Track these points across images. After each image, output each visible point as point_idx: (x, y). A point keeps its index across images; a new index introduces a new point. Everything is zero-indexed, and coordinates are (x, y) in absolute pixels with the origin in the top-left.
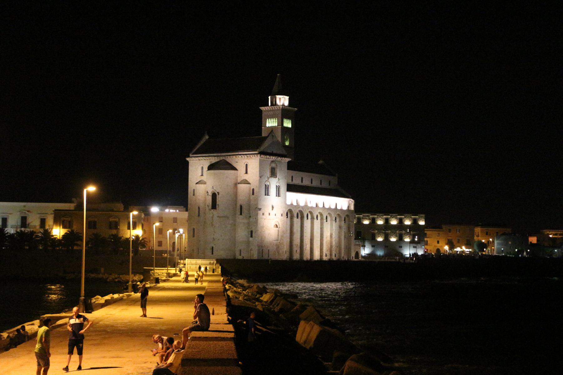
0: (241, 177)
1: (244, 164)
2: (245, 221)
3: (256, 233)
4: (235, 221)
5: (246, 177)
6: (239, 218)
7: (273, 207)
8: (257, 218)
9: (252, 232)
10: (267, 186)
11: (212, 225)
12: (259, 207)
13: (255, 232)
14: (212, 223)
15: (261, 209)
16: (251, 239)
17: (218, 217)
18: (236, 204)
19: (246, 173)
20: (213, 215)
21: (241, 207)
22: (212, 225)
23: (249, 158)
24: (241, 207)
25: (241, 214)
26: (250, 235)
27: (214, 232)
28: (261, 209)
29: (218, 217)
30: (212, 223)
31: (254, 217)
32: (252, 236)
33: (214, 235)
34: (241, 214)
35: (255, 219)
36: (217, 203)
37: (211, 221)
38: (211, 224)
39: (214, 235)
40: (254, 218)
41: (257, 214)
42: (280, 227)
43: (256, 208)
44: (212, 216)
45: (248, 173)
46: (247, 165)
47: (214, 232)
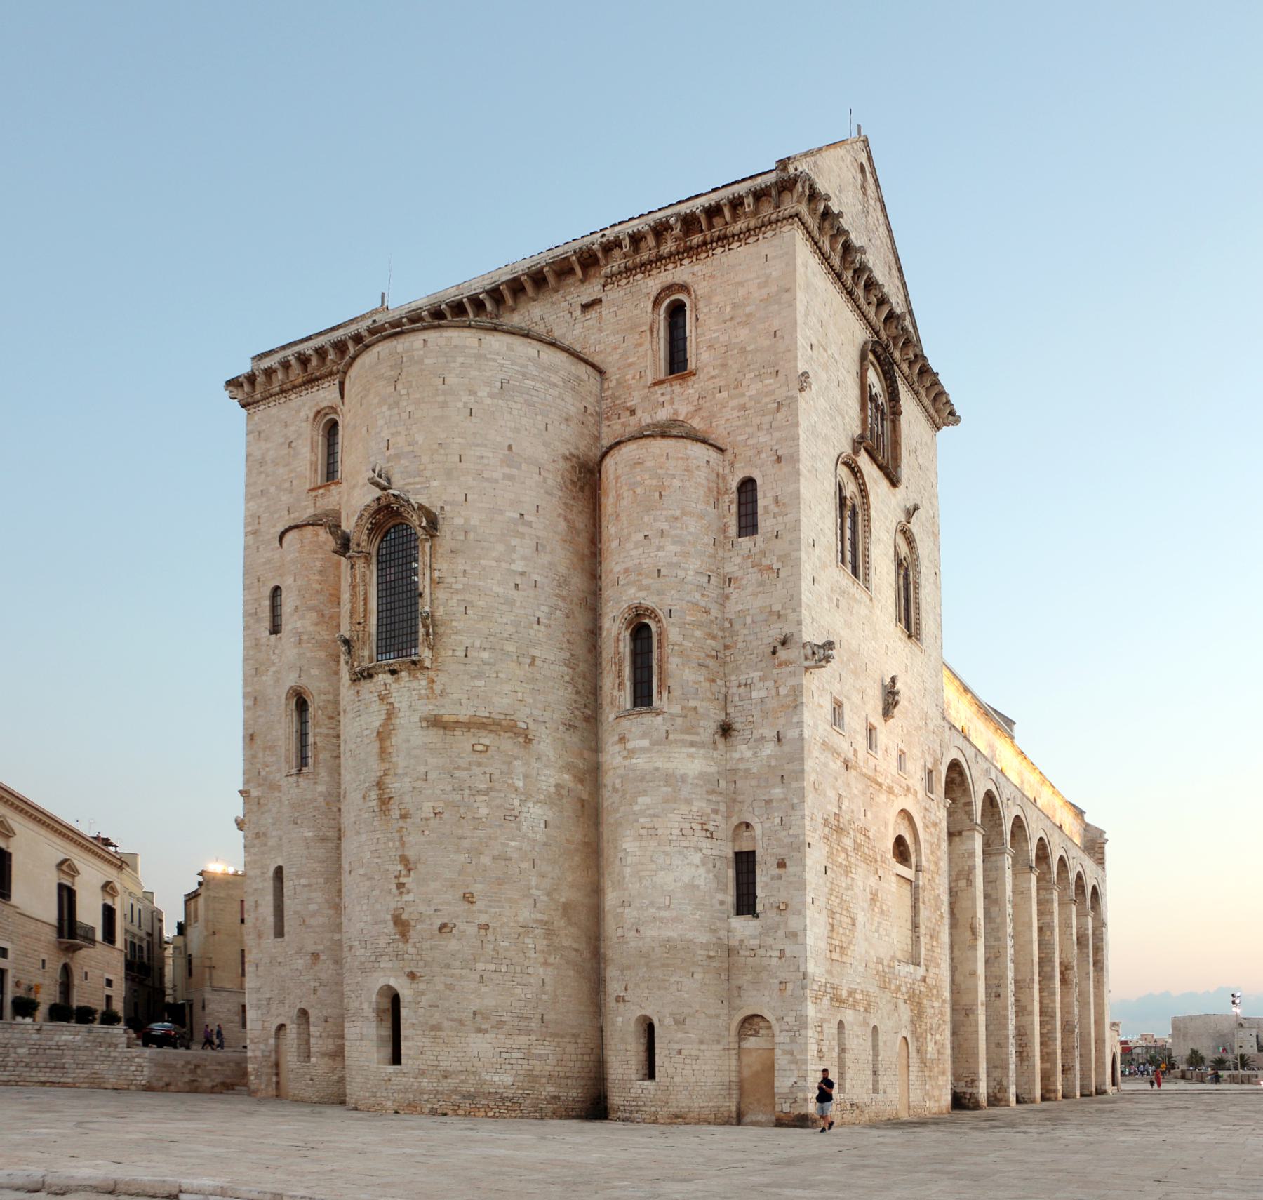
0: (633, 412)
1: (657, 303)
3: (791, 869)
6: (623, 739)
8: (792, 734)
9: (745, 863)
11: (384, 802)
12: (806, 638)
13: (782, 865)
14: (380, 785)
15: (829, 645)
16: (743, 926)
17: (435, 722)
18: (594, 632)
19: (677, 363)
20: (390, 715)
21: (641, 632)
22: (385, 802)
23: (696, 239)
24: (641, 632)
25: (642, 696)
26: (730, 898)
27: (404, 860)
28: (829, 645)
30: (380, 785)
31: (770, 733)
32: (746, 903)
33: (400, 886)
34: (642, 696)
35: (769, 749)
36: (425, 606)
37: (376, 767)
38: (374, 794)
39: (400, 886)
40: (762, 739)
41: (797, 691)
43: (784, 643)
44: (377, 721)
45: (691, 365)
46: (676, 313)
47: (404, 860)
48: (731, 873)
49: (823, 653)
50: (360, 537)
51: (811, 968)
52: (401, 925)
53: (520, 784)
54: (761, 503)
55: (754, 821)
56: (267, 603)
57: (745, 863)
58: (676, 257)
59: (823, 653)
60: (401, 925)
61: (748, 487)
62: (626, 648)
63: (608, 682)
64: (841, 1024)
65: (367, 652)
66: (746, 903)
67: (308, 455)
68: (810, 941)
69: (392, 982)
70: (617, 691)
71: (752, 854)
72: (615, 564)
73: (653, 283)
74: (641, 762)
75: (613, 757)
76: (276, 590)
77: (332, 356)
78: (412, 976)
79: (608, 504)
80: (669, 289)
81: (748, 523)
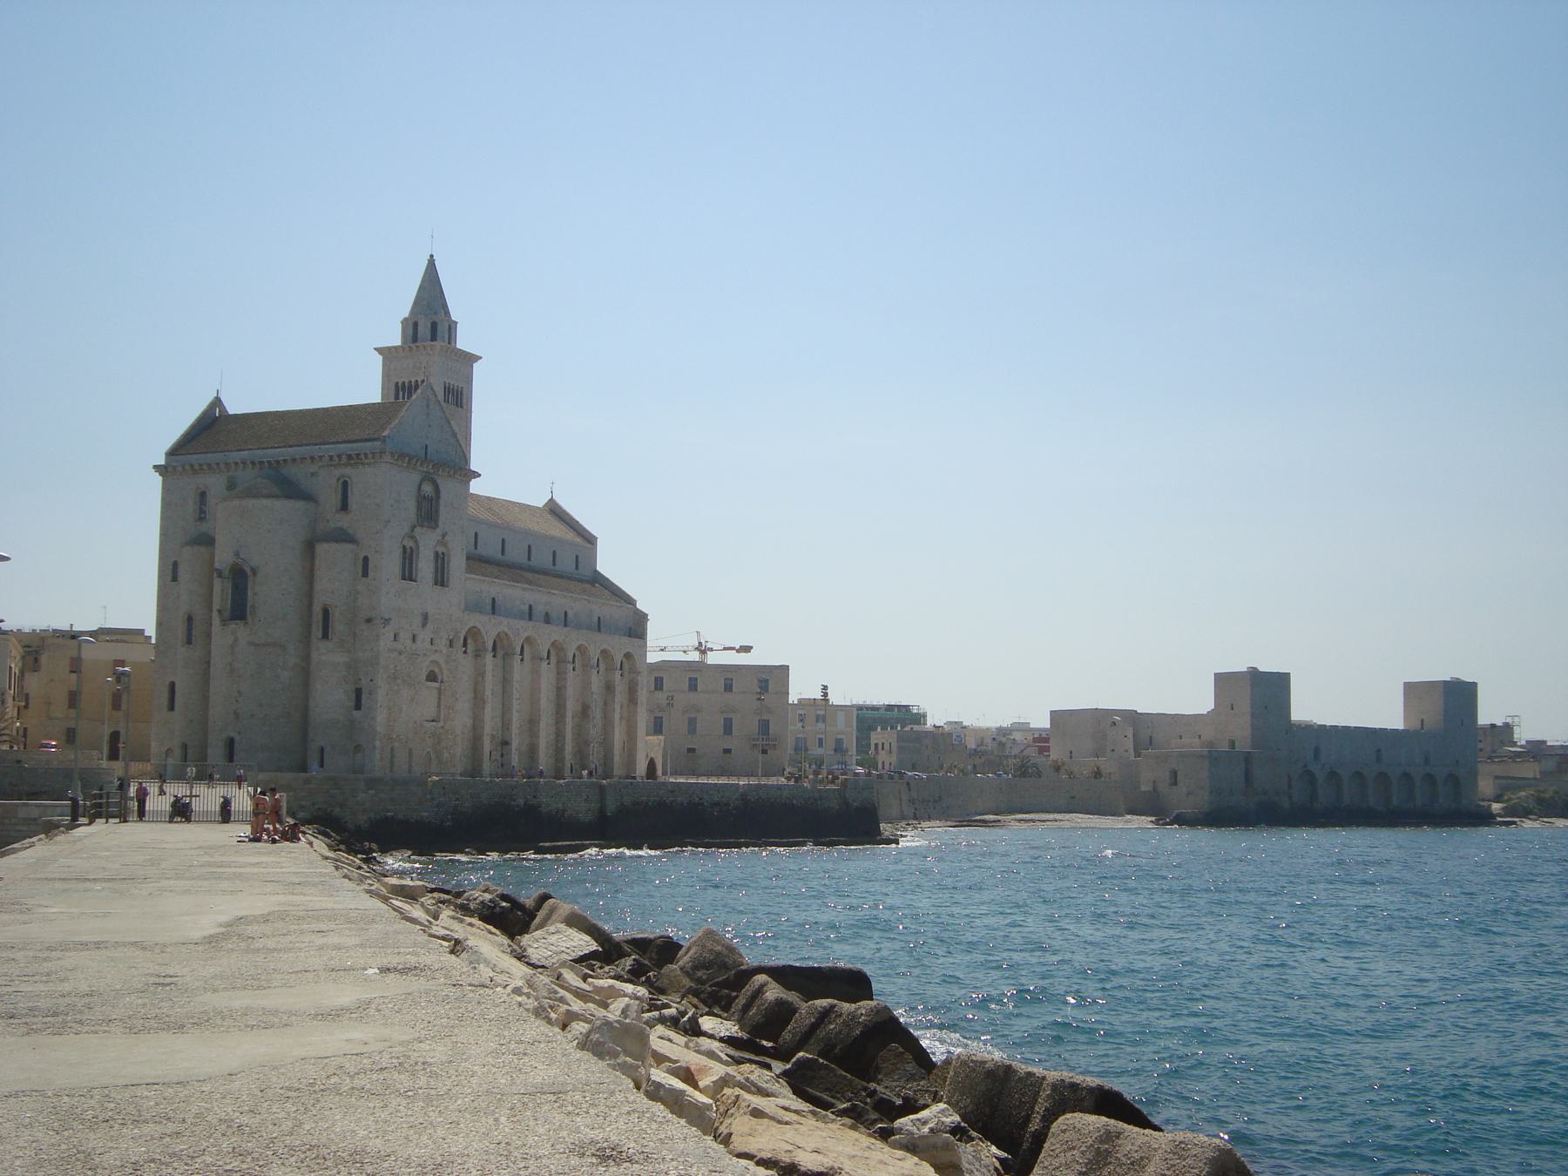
0: (328, 521)
1: (338, 480)
2: (341, 658)
4: (307, 658)
5: (343, 521)
7: (425, 617)
9: (358, 692)
10: (408, 551)
17: (252, 644)
18: (310, 605)
19: (344, 507)
20: (236, 639)
21: (326, 613)
23: (352, 462)
24: (326, 613)
25: (325, 636)
26: (352, 704)
27: (238, 691)
28: (390, 619)
29: (252, 644)
32: (358, 706)
34: (325, 636)
39: (237, 701)
42: (445, 679)
46: (345, 484)
48: (354, 695)
49: (387, 621)
50: (226, 573)
51: (379, 729)
52: (237, 715)
53: (281, 664)
54: (370, 567)
55: (362, 678)
56: (171, 567)
57: (358, 692)
58: (346, 465)
59: (387, 621)
60: (237, 715)
61: (366, 559)
62: (320, 617)
63: (314, 627)
64: (392, 749)
65: (227, 614)
66: (358, 706)
67: (191, 507)
68: (379, 720)
69: (232, 735)
70: (317, 631)
71: (361, 689)
72: (320, 585)
73: (338, 472)
74: (324, 658)
75: (314, 655)
76: (175, 564)
77: (205, 467)
78: (239, 733)
79: (317, 562)
80: (343, 476)
81: (365, 574)
